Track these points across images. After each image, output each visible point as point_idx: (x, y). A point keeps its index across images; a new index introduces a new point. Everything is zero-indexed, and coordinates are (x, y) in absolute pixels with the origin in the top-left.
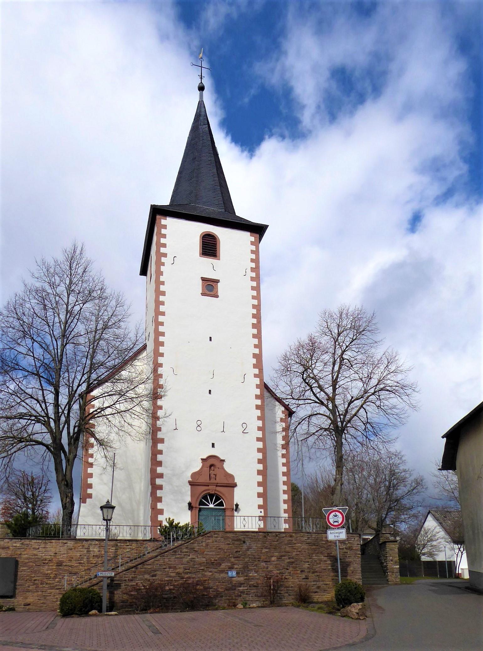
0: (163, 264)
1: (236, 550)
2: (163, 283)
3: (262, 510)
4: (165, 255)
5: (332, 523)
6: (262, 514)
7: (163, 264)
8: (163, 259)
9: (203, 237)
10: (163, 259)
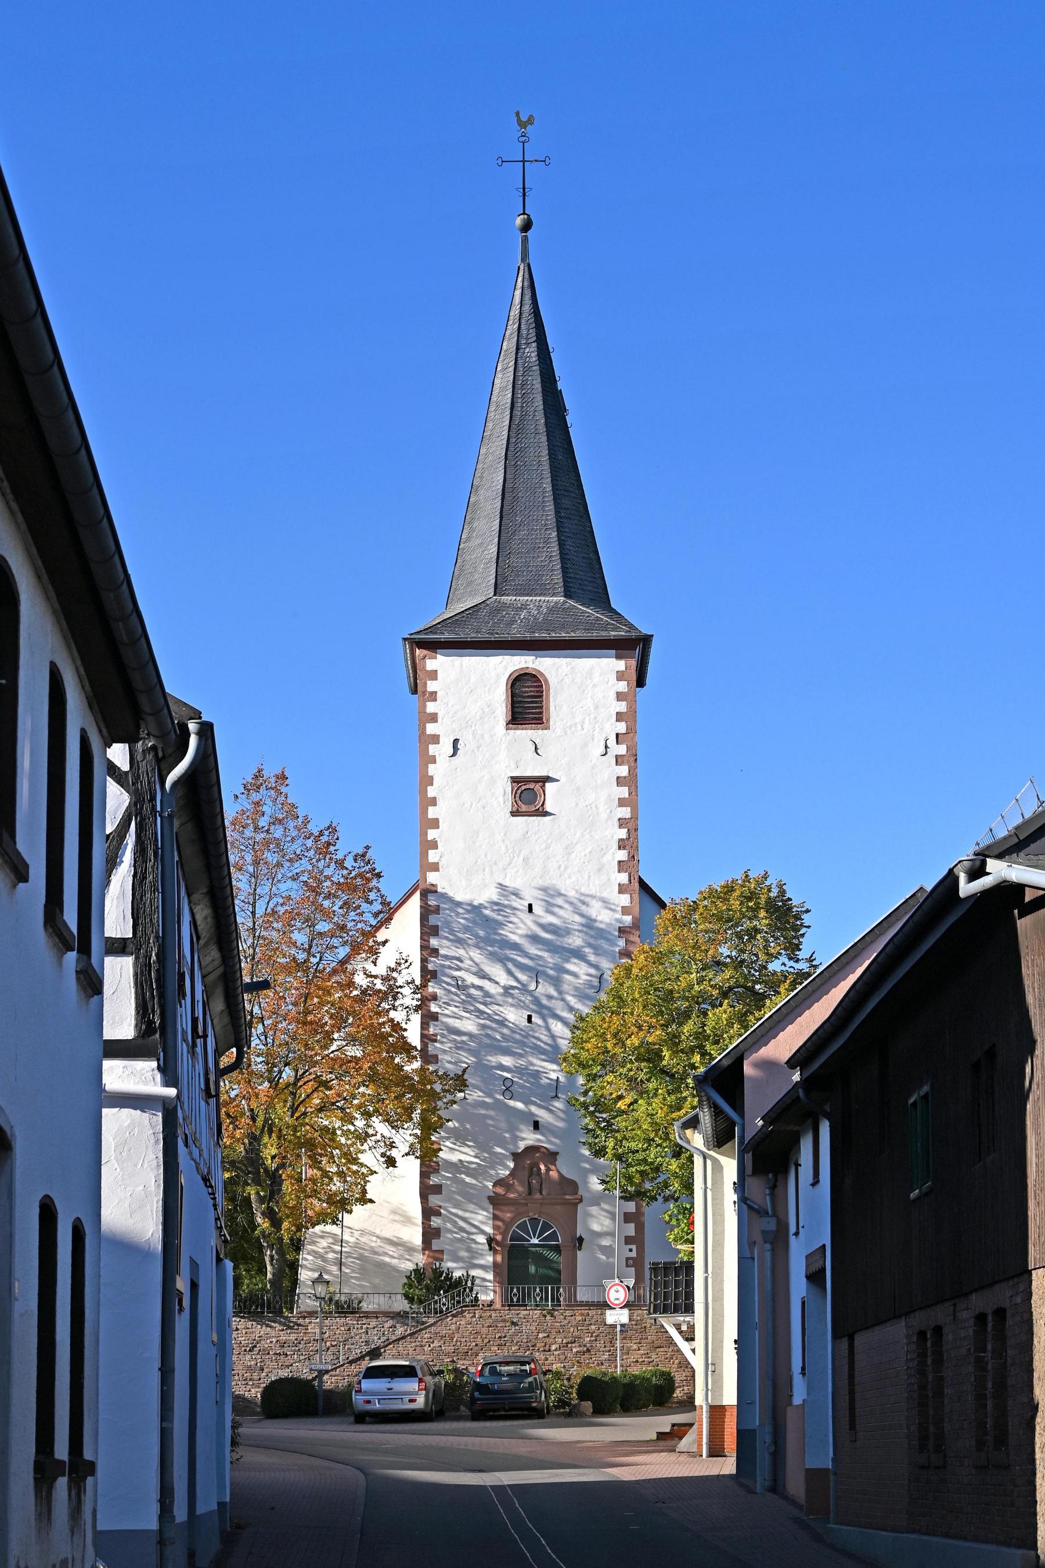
0: (433, 760)
1: (499, 1335)
2: (433, 802)
3: (634, 1247)
4: (435, 739)
5: (613, 1301)
6: (634, 1254)
7: (433, 760)
8: (432, 749)
9: (513, 685)
10: (432, 749)
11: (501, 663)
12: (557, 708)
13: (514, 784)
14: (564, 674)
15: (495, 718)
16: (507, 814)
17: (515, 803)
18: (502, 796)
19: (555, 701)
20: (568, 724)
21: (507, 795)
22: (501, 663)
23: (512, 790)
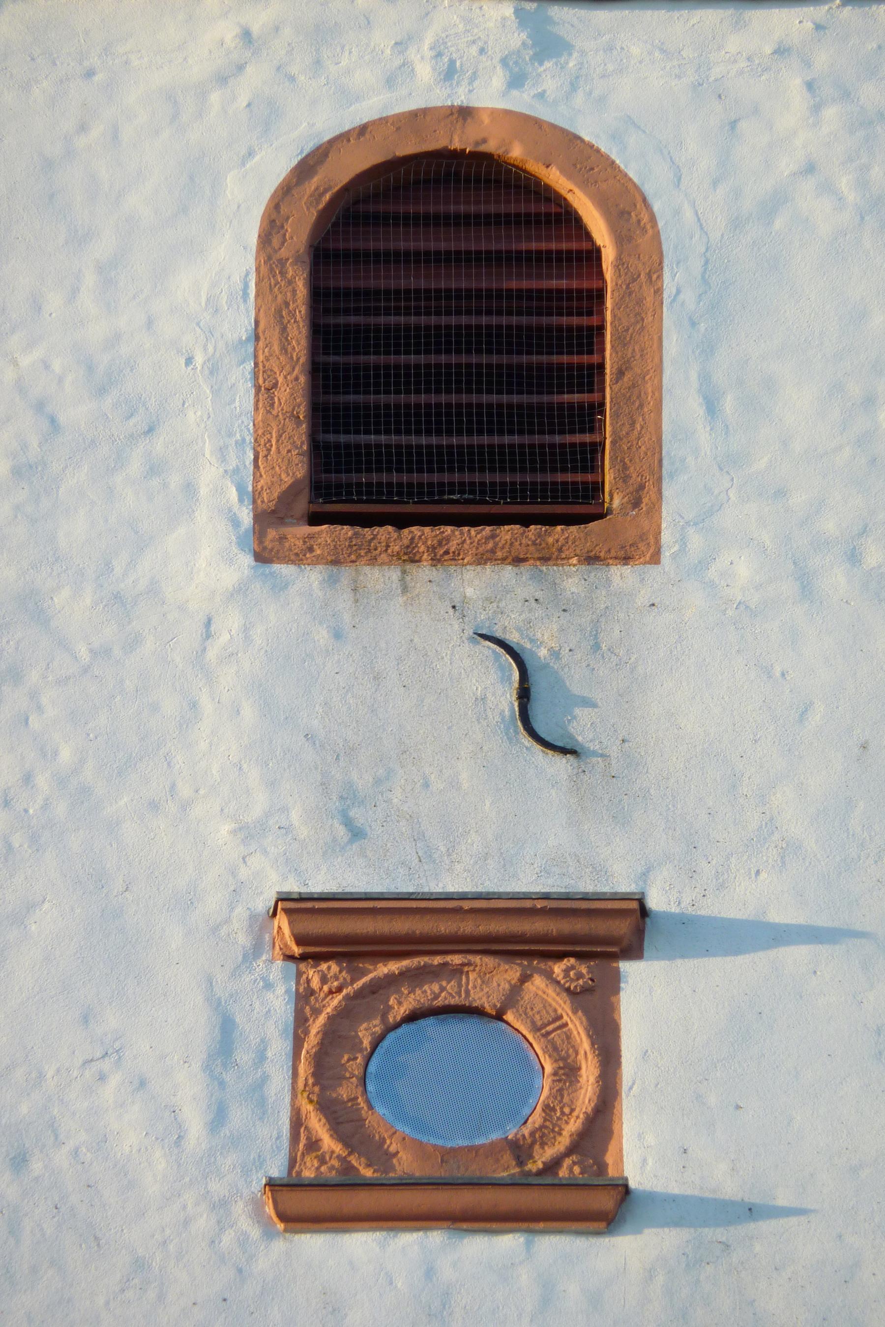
11: (222, 79)
12: (728, 404)
13: (313, 975)
14: (786, 165)
15: (154, 469)
16: (240, 1211)
17: (318, 1126)
18: (225, 1297)
19: (708, 349)
20: (829, 525)
21: (244, 1056)
22: (222, 79)
23: (301, 1022)
